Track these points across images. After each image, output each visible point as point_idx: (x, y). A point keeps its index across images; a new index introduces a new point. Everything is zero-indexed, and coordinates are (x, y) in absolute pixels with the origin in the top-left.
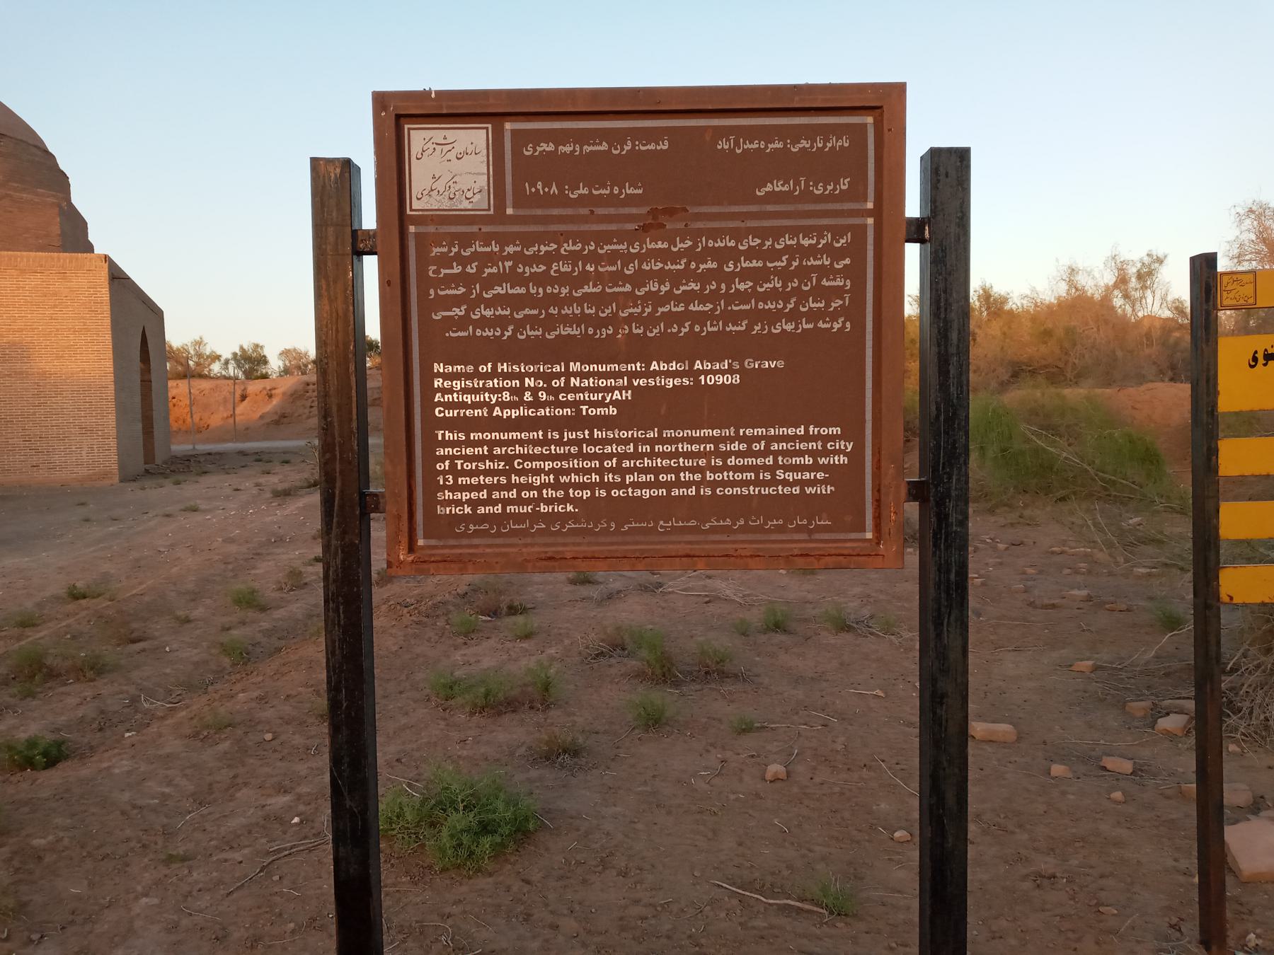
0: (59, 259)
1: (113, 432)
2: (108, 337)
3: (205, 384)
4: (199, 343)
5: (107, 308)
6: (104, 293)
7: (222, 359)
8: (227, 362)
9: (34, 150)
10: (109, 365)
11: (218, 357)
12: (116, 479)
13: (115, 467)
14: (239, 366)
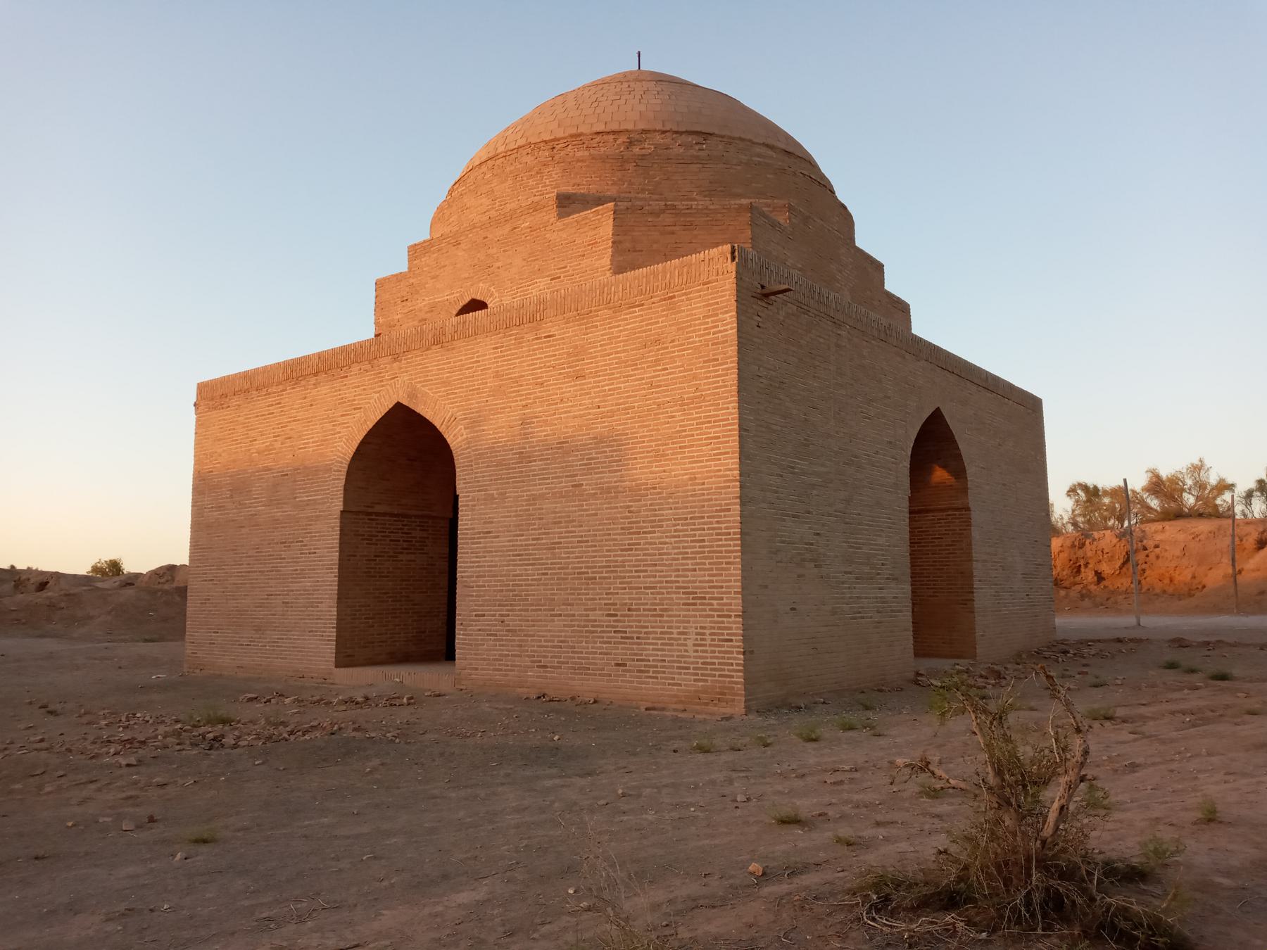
0: (664, 272)
1: (737, 603)
2: (730, 409)
3: (1204, 526)
4: (1197, 468)
5: (732, 350)
7: (1241, 489)
8: (1249, 495)
9: (763, 150)
10: (732, 463)
11: (1231, 487)
12: (739, 708)
13: (739, 678)
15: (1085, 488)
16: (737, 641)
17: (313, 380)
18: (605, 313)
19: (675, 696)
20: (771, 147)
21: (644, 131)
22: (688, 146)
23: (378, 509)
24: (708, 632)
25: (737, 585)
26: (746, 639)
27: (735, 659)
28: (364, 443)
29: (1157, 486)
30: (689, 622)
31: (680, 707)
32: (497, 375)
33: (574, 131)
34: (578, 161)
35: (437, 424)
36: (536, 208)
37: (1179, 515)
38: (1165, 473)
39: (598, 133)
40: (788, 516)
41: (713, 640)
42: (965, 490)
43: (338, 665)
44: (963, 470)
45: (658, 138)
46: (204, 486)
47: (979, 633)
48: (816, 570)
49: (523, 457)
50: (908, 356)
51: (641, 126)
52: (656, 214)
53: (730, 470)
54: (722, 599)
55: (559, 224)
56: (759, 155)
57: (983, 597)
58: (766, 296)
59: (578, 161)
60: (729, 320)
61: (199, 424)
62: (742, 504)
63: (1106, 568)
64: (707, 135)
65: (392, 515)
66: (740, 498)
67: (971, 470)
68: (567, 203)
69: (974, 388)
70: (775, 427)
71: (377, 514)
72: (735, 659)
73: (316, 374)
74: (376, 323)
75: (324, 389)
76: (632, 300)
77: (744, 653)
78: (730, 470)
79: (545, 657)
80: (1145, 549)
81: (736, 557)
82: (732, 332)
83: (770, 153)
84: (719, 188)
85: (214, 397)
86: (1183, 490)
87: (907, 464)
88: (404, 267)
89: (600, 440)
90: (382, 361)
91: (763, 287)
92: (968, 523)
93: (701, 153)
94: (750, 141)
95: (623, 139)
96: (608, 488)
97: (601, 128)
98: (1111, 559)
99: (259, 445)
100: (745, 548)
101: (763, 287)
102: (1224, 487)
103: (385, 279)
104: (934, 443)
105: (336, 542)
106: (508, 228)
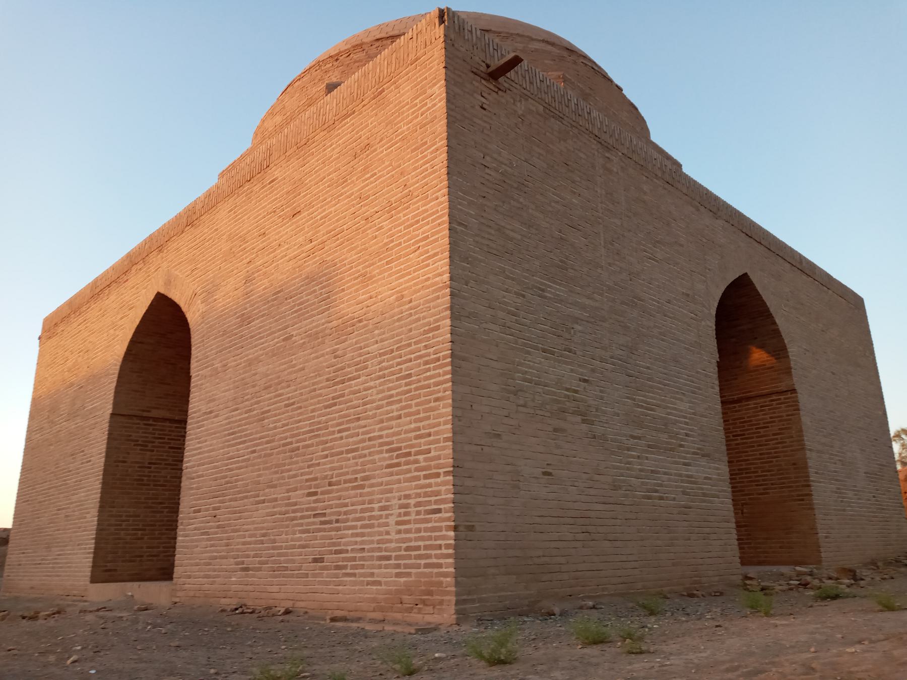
5: (441, 126)
10: (439, 268)
12: (447, 615)
19: (374, 600)
23: (155, 413)
24: (412, 502)
25: (446, 429)
26: (458, 507)
27: (444, 538)
28: (133, 342)
30: (390, 491)
31: (378, 615)
35: (182, 305)
39: (378, 40)
40: (537, 348)
41: (418, 513)
42: (788, 371)
43: (94, 580)
44: (784, 349)
47: (821, 535)
48: (584, 427)
50: (702, 209)
53: (440, 275)
54: (429, 451)
57: (823, 492)
59: (355, 62)
60: (439, 90)
62: (453, 317)
66: (451, 308)
67: (793, 350)
69: (788, 265)
70: (512, 234)
71: (156, 419)
72: (444, 538)
73: (109, 286)
76: (345, 112)
77: (455, 529)
78: (440, 275)
79: (248, 556)
81: (446, 390)
83: (549, 48)
87: (712, 323)
89: (310, 279)
91: (488, 66)
94: (528, 37)
96: (317, 333)
101: (488, 66)
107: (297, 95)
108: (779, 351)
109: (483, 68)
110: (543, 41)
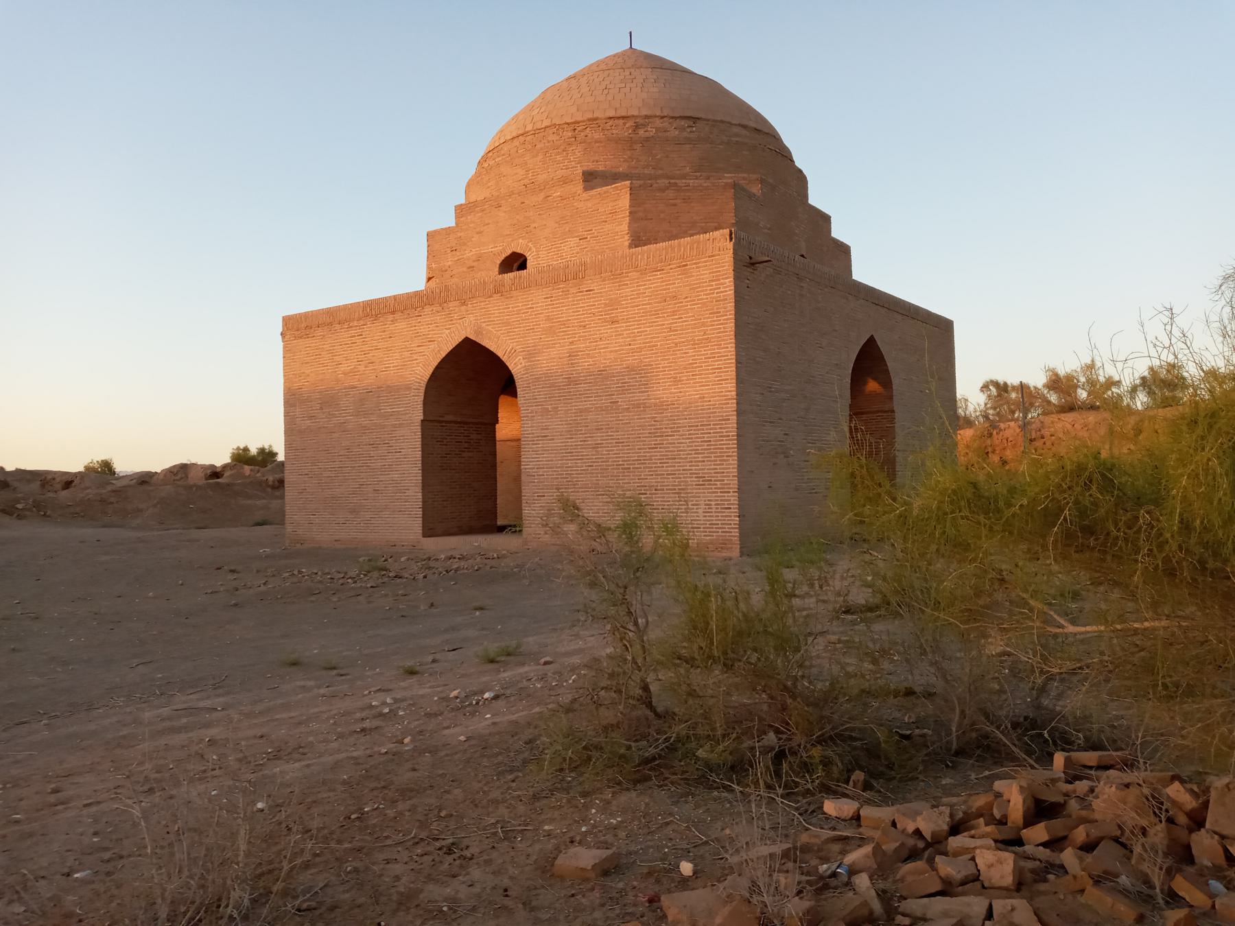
1: (734, 483)
2: (731, 348)
3: (1092, 417)
4: (1091, 367)
5: (731, 306)
6: (727, 286)
8: (1134, 390)
10: (730, 387)
11: (1118, 383)
12: (735, 553)
13: (736, 533)
14: (1150, 393)
15: (996, 384)
16: (735, 509)
17: (390, 317)
18: (634, 275)
20: (745, 127)
21: (647, 117)
22: (682, 129)
26: (741, 507)
29: (1057, 383)
32: (548, 319)
33: (590, 116)
34: (596, 142)
35: (500, 354)
36: (565, 181)
37: (1070, 408)
38: (1061, 373)
42: (891, 398)
44: (890, 382)
45: (658, 122)
46: (292, 400)
49: (570, 381)
51: (644, 112)
52: (662, 190)
55: (585, 195)
56: (737, 135)
58: (753, 264)
59: (596, 142)
61: (287, 350)
62: (738, 415)
63: (1009, 454)
64: (695, 119)
65: (456, 422)
68: (591, 179)
69: (899, 317)
73: (393, 313)
74: (429, 268)
75: (401, 325)
80: (1043, 437)
82: (730, 292)
83: (744, 132)
84: (703, 161)
85: (298, 329)
86: (1077, 386)
88: (451, 222)
89: (631, 369)
90: (451, 304)
92: (892, 420)
93: (692, 135)
95: (630, 123)
97: (612, 114)
98: (1014, 446)
99: (344, 368)
100: (740, 446)
102: (1111, 383)
103: (435, 232)
104: (869, 361)
105: (419, 445)
106: (542, 195)
107: (540, 157)
108: (887, 383)
109: (748, 260)
110: (739, 125)
